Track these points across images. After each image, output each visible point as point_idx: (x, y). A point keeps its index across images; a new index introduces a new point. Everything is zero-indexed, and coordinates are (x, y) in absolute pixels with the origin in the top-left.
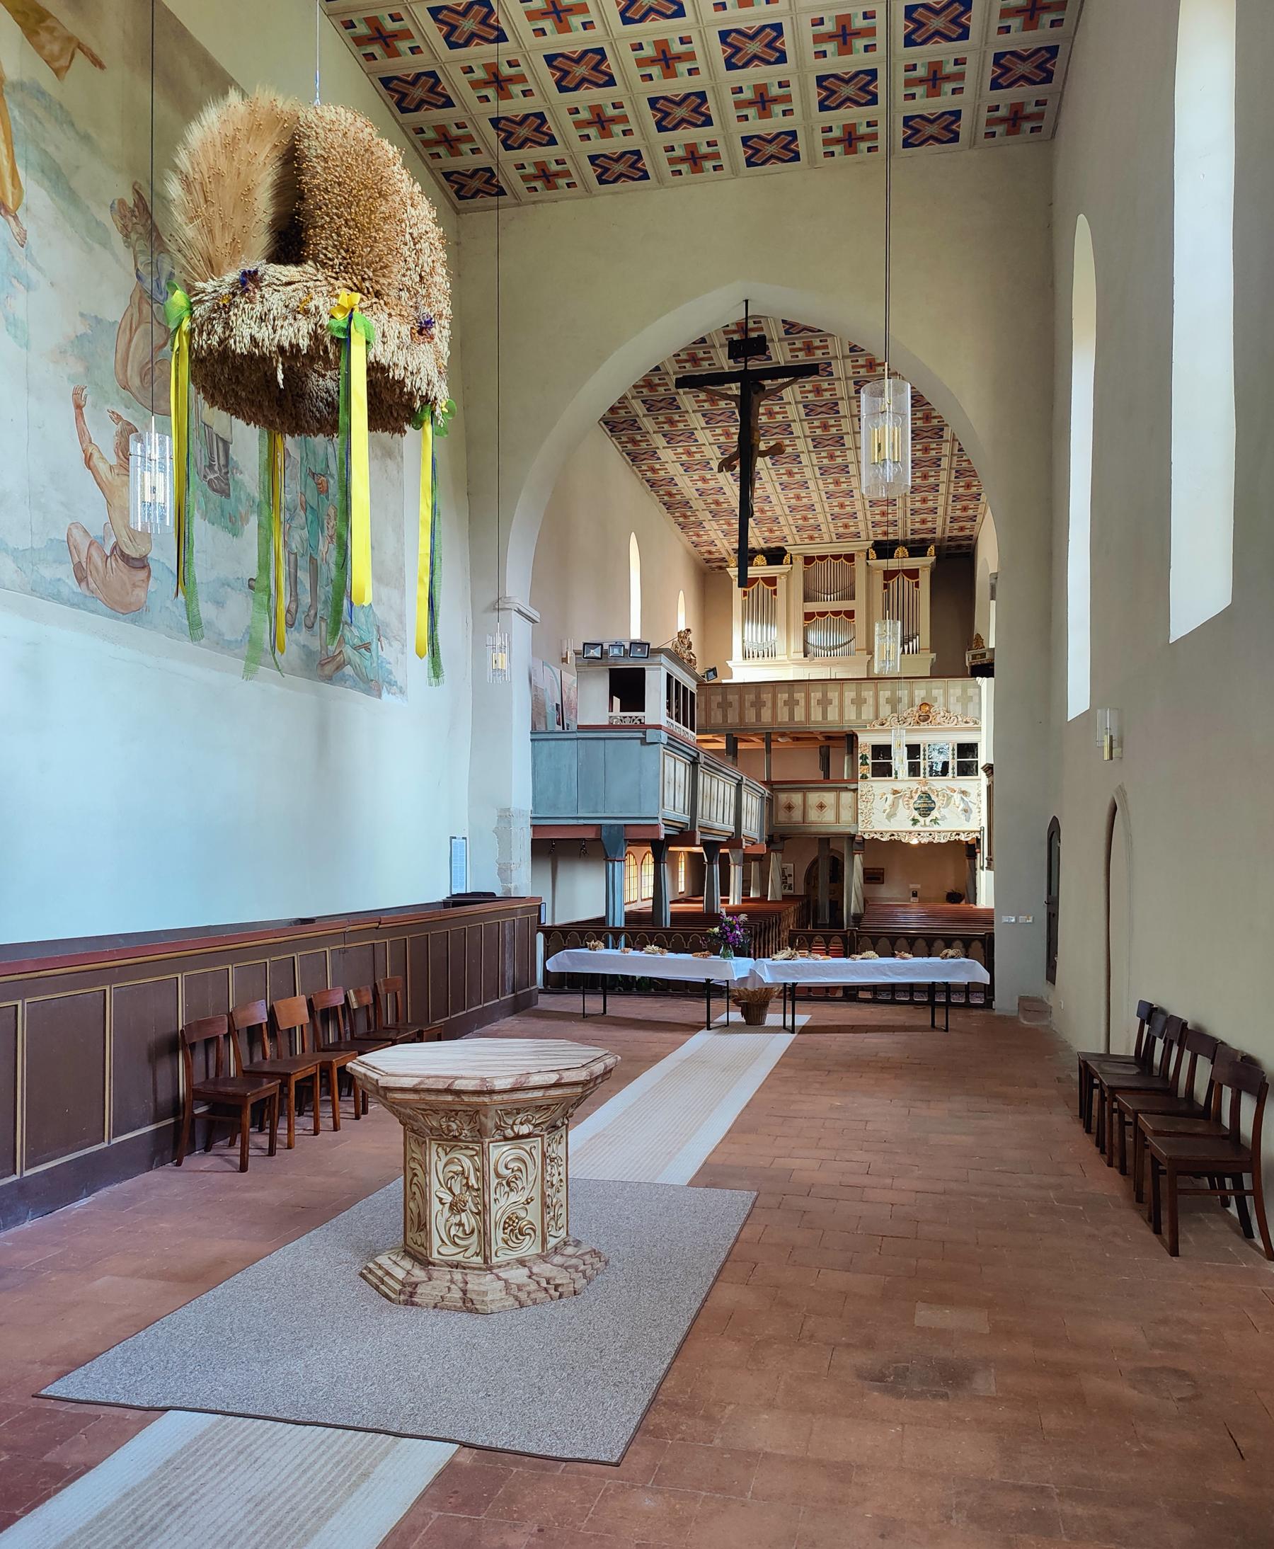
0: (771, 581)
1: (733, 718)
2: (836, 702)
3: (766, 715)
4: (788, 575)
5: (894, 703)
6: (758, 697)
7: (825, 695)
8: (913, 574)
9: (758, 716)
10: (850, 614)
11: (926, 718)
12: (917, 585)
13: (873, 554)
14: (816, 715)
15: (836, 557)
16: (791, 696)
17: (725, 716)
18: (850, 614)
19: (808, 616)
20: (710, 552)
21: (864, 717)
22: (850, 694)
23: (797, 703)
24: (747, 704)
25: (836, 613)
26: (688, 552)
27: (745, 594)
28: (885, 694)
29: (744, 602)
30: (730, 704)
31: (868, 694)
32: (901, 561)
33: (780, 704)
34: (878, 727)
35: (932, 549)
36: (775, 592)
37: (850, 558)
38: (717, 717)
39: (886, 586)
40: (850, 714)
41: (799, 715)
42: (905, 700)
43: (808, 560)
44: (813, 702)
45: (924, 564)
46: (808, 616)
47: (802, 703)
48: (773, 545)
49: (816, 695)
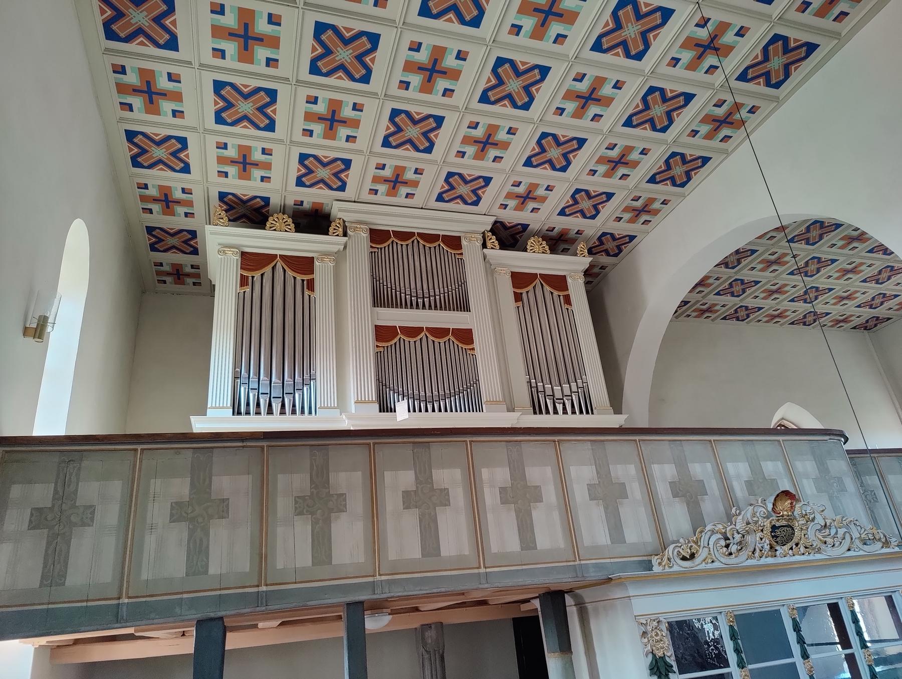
0: (304, 265)
1: (229, 554)
2: (550, 494)
3: (348, 541)
4: (339, 257)
5: (689, 492)
6: (320, 478)
7: (517, 471)
8: (558, 282)
9: (322, 543)
10: (465, 336)
11: (782, 534)
12: (567, 300)
13: (492, 240)
14: (503, 536)
15: (430, 238)
16: (424, 478)
17: (198, 551)
18: (465, 336)
19: (383, 333)
20: (167, 201)
21: (631, 536)
22: (582, 474)
23: (444, 498)
24: (283, 505)
25: (439, 333)
26: (115, 178)
27: (244, 281)
28: (664, 473)
29: (241, 300)
30: (223, 508)
31: (625, 472)
32: (536, 260)
33: (392, 501)
34: (680, 566)
35: (581, 247)
36: (311, 285)
37: (454, 242)
38: (164, 557)
39: (518, 297)
40: (594, 530)
41: (454, 538)
42: (713, 486)
43: (378, 236)
44: (490, 497)
45: (572, 266)
46: (383, 333)
47: (458, 496)
48: (311, 196)
49: (495, 476)
